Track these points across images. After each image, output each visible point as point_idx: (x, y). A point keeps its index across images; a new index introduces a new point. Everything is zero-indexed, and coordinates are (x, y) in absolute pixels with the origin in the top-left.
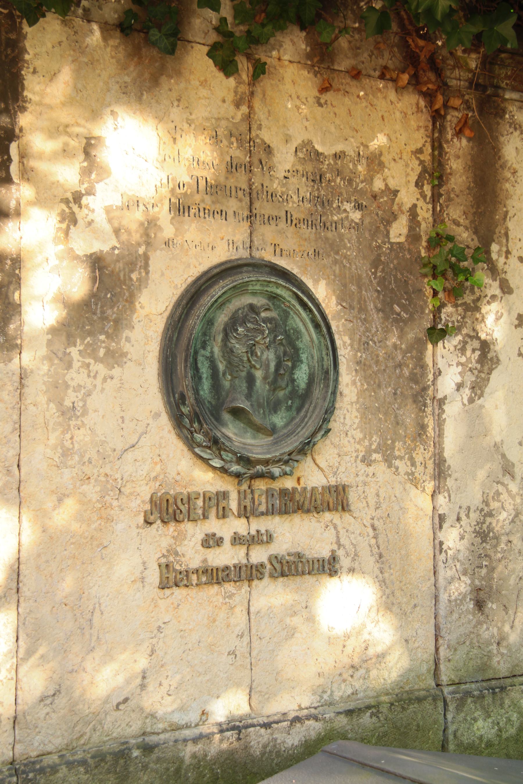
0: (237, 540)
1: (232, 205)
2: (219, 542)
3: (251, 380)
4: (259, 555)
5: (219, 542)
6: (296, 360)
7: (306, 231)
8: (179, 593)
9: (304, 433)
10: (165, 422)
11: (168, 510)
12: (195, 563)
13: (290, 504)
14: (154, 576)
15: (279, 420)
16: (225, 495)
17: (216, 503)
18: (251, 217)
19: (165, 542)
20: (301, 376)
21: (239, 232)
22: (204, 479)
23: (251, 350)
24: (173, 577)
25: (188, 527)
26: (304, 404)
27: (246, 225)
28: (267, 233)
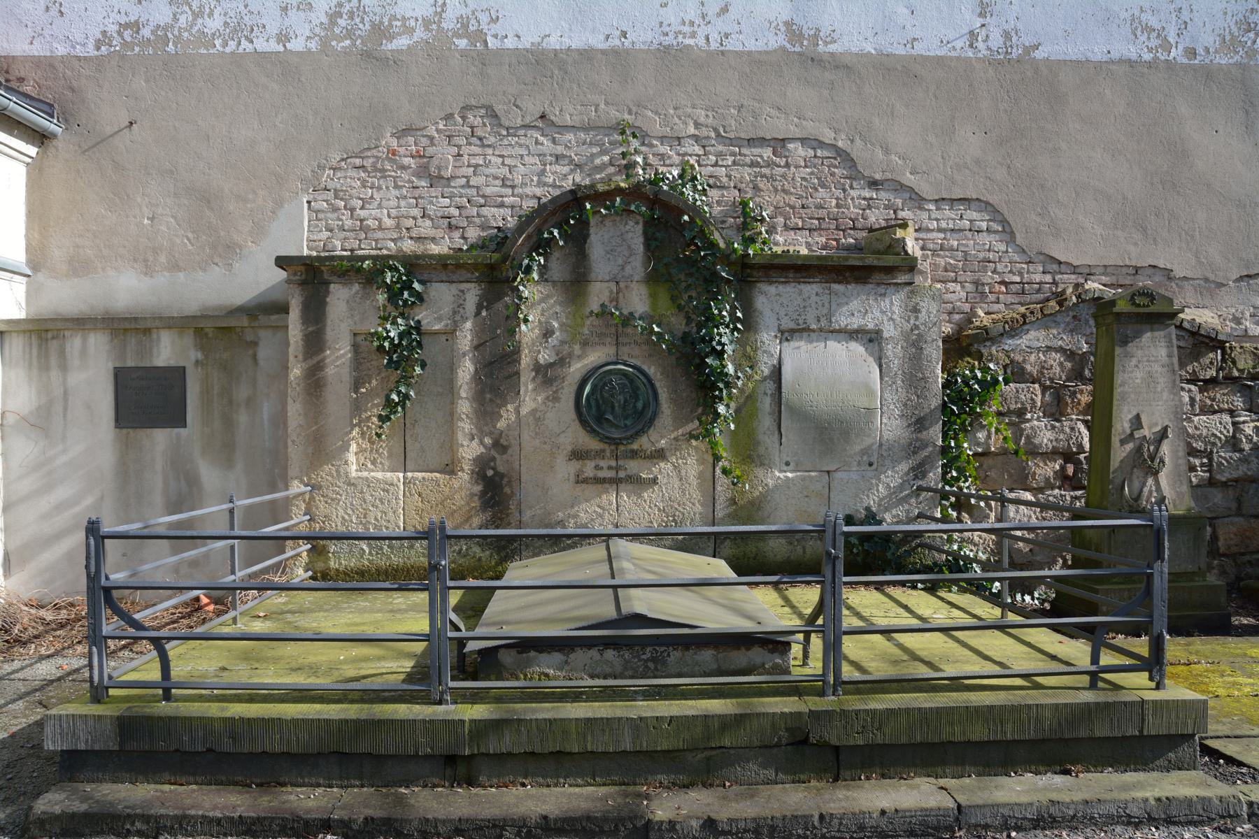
0: (610, 468)
1: (609, 339)
2: (602, 468)
3: (613, 407)
4: (622, 474)
5: (602, 468)
6: (637, 399)
7: (644, 347)
8: (584, 485)
9: (640, 427)
10: (577, 422)
11: (578, 455)
12: (591, 475)
13: (634, 455)
14: (572, 478)
15: (628, 422)
16: (604, 451)
17: (600, 454)
18: (617, 344)
19: (578, 467)
20: (640, 405)
21: (611, 350)
22: (594, 444)
23: (612, 396)
24: (580, 480)
25: (588, 462)
26: (643, 418)
27: (614, 348)
28: (625, 350)
